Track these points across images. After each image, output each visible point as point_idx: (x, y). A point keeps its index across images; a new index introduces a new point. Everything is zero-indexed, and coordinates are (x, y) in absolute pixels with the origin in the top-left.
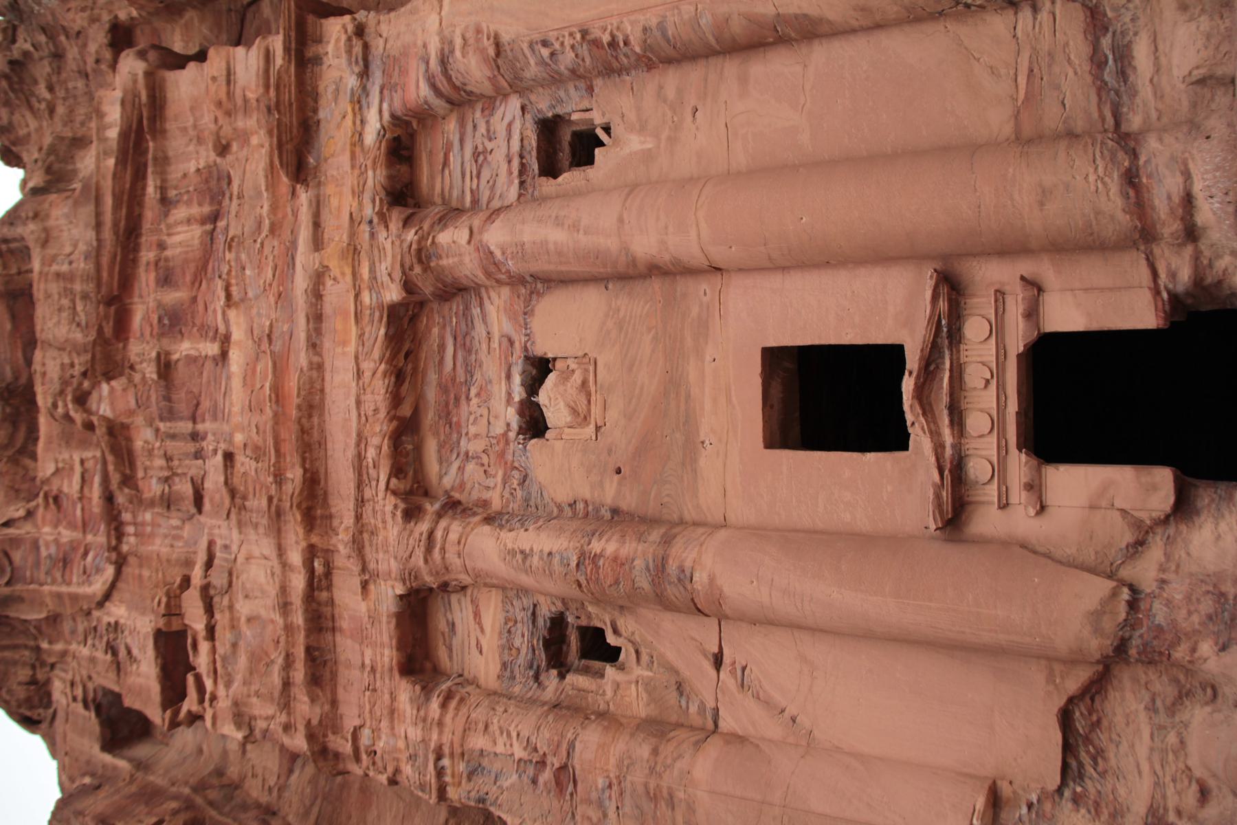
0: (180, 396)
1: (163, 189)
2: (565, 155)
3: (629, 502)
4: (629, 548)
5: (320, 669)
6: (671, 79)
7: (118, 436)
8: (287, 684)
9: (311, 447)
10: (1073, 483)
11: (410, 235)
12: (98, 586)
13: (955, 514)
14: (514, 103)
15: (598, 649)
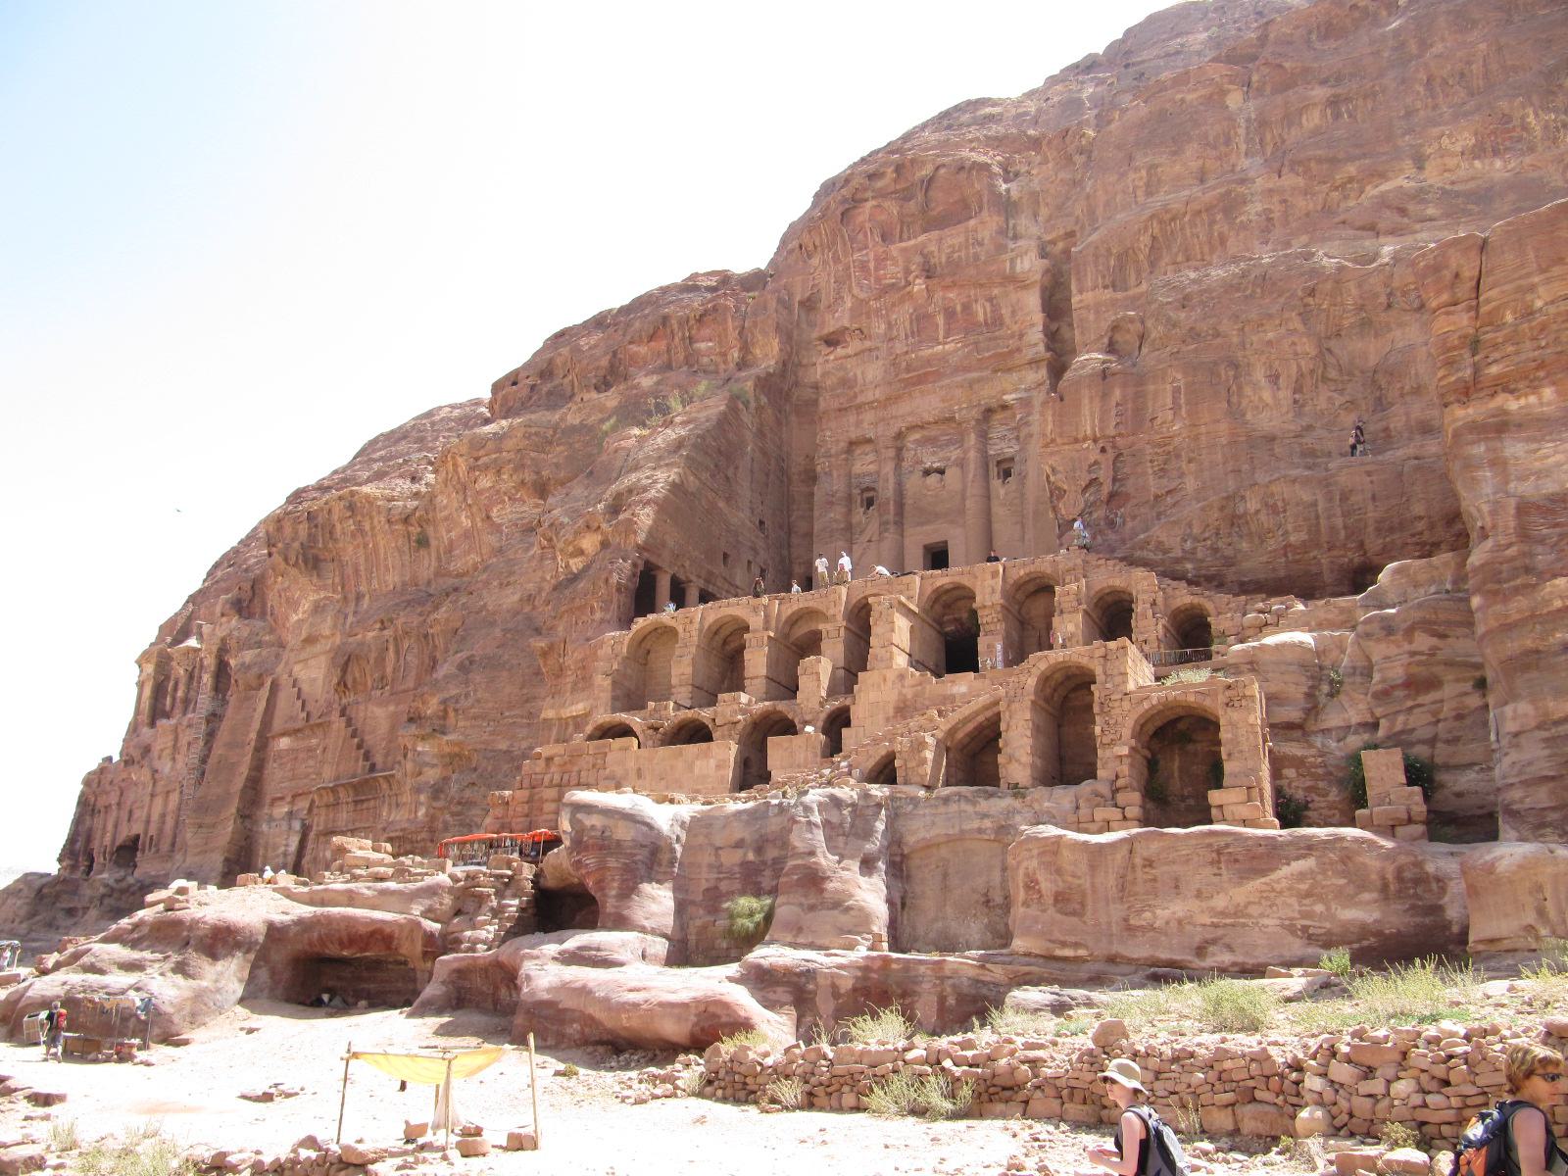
2: (1005, 466)
3: (907, 508)
4: (892, 512)
11: (973, 423)
12: (856, 291)
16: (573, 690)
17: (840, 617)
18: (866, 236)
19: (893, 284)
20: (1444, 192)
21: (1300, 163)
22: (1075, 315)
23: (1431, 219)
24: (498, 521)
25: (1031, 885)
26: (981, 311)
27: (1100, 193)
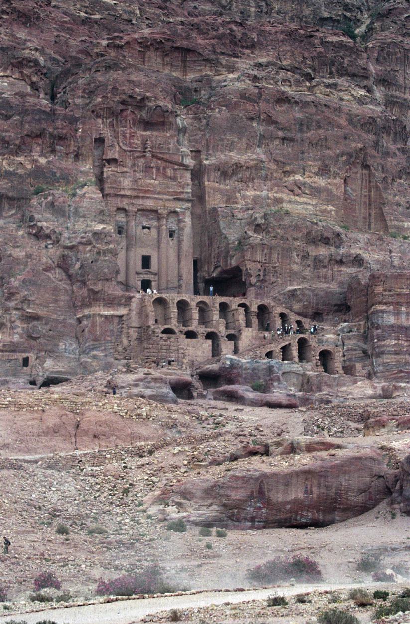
0: (148, 169)
1: (176, 169)
5: (116, 195)
7: (145, 156)
8: (113, 188)
9: (143, 197)
12: (121, 144)
13: (137, 273)
14: (177, 228)
15: (120, 232)
16: (104, 306)
17: (218, 307)
18: (126, 121)
19: (136, 148)
20: (310, 186)
21: (275, 160)
22: (206, 189)
23: (307, 194)
26: (169, 172)
27: (212, 141)
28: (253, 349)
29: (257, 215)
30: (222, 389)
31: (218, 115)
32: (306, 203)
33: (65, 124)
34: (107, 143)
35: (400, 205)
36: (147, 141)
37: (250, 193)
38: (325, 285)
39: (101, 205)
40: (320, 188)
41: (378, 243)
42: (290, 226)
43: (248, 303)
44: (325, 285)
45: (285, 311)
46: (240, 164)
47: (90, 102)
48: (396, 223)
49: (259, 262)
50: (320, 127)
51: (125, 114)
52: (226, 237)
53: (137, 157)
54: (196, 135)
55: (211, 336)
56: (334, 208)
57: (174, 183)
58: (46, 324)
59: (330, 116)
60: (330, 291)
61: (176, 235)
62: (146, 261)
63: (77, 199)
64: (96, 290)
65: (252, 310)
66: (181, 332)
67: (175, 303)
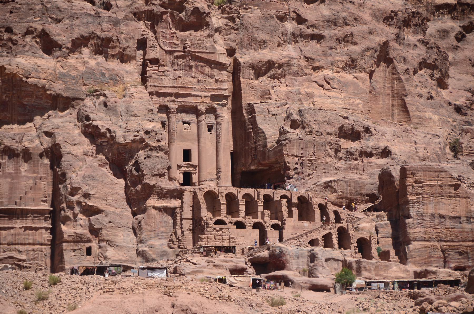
6: (215, 141)
10: (181, 176)
17: (262, 199)
20: (338, 81)
21: (306, 58)
23: (335, 88)
24: (26, 103)
25: (365, 267)
28: (297, 237)
29: (292, 111)
30: (272, 274)
31: (251, 15)
32: (335, 98)
33: (110, 26)
34: (149, 43)
35: (421, 97)
36: (186, 41)
37: (283, 89)
38: (357, 176)
39: (149, 104)
40: (348, 83)
41: (403, 135)
42: (323, 122)
43: (289, 196)
44: (357, 176)
45: (323, 202)
46: (272, 61)
47: (131, 5)
48: (418, 114)
49: (296, 156)
50: (346, 24)
51: (164, 16)
52: (263, 132)
53: (177, 57)
54: (230, 34)
55: (256, 226)
56: (361, 102)
57: (211, 81)
58: (106, 216)
59: (355, 12)
60: (362, 183)
61: (214, 130)
62: (187, 155)
63: (127, 99)
64: (151, 184)
65: (293, 202)
66: (231, 223)
67: (224, 196)
